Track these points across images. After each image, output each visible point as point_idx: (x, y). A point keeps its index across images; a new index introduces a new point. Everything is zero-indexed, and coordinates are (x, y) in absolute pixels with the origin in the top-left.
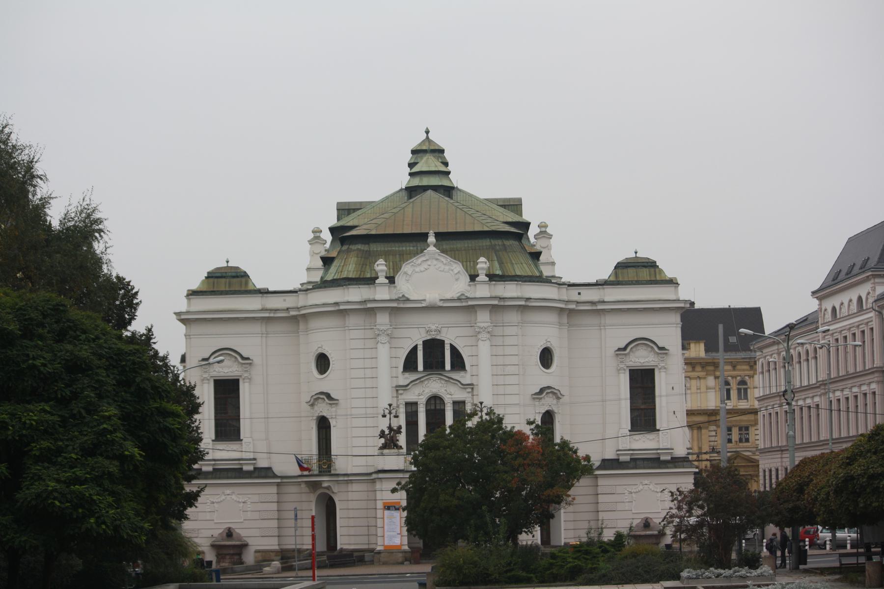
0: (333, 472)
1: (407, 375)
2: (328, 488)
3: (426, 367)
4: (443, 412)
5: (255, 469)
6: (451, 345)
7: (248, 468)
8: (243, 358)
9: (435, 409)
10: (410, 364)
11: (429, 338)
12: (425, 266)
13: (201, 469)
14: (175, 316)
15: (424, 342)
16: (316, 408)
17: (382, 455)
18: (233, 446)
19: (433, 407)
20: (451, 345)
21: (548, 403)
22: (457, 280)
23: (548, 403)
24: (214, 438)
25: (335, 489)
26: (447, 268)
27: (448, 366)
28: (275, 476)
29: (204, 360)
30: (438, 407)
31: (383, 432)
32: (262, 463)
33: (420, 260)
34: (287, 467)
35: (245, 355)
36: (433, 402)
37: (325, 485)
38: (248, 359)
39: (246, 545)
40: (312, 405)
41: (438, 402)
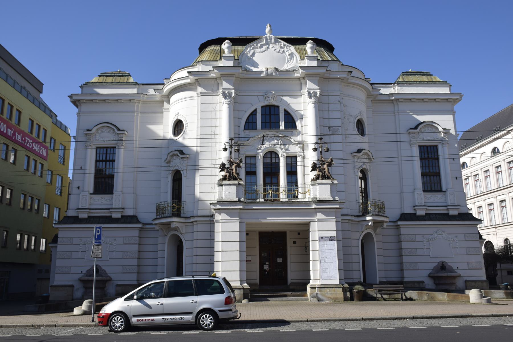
0: (182, 215)
1: (247, 132)
2: (176, 229)
3: (264, 127)
4: (278, 165)
5: (122, 216)
6: (285, 110)
7: (116, 215)
8: (119, 130)
9: (271, 163)
10: (250, 123)
11: (266, 103)
12: (265, 47)
13: (78, 216)
14: (69, 99)
15: (262, 107)
16: (172, 164)
17: (222, 185)
18: (107, 197)
19: (269, 161)
20: (285, 110)
21: (363, 162)
22: (291, 59)
23: (363, 162)
24: (92, 192)
25: (183, 230)
26: (282, 50)
27: (282, 126)
28: (138, 222)
29: (88, 130)
30: (273, 161)
31: (223, 165)
32: (130, 212)
33: (259, 45)
34: (147, 213)
35: (121, 128)
36: (269, 156)
37: (174, 225)
38: (123, 130)
39: (110, 280)
40: (169, 162)
41: (273, 156)
